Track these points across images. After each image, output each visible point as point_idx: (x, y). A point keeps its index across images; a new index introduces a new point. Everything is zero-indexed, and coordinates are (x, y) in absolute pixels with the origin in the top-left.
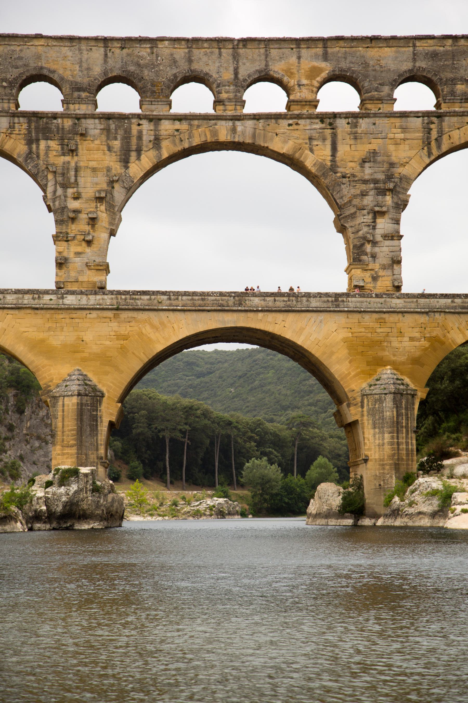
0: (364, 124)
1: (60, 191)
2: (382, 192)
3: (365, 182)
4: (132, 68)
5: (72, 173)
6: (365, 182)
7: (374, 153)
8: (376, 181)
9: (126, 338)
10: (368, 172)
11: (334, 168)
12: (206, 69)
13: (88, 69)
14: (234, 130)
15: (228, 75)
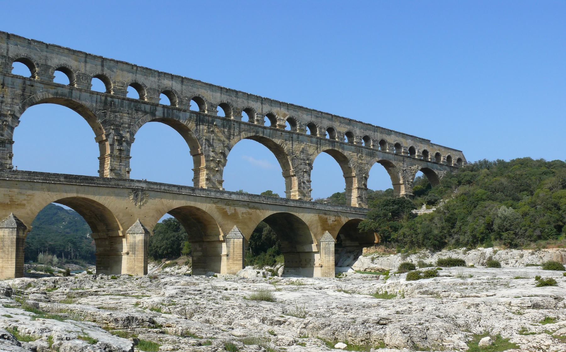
0: (300, 137)
1: (207, 148)
2: (306, 164)
3: (301, 159)
4: (229, 101)
5: (211, 141)
6: (301, 159)
7: (303, 149)
8: (304, 160)
9: (251, 214)
10: (302, 156)
11: (292, 153)
12: (253, 107)
13: (215, 98)
14: (263, 132)
15: (260, 111)
